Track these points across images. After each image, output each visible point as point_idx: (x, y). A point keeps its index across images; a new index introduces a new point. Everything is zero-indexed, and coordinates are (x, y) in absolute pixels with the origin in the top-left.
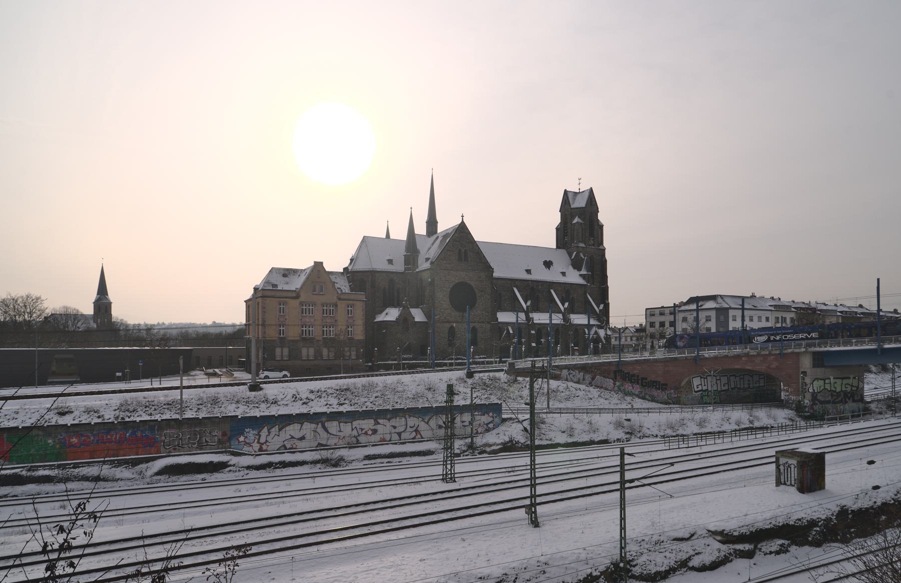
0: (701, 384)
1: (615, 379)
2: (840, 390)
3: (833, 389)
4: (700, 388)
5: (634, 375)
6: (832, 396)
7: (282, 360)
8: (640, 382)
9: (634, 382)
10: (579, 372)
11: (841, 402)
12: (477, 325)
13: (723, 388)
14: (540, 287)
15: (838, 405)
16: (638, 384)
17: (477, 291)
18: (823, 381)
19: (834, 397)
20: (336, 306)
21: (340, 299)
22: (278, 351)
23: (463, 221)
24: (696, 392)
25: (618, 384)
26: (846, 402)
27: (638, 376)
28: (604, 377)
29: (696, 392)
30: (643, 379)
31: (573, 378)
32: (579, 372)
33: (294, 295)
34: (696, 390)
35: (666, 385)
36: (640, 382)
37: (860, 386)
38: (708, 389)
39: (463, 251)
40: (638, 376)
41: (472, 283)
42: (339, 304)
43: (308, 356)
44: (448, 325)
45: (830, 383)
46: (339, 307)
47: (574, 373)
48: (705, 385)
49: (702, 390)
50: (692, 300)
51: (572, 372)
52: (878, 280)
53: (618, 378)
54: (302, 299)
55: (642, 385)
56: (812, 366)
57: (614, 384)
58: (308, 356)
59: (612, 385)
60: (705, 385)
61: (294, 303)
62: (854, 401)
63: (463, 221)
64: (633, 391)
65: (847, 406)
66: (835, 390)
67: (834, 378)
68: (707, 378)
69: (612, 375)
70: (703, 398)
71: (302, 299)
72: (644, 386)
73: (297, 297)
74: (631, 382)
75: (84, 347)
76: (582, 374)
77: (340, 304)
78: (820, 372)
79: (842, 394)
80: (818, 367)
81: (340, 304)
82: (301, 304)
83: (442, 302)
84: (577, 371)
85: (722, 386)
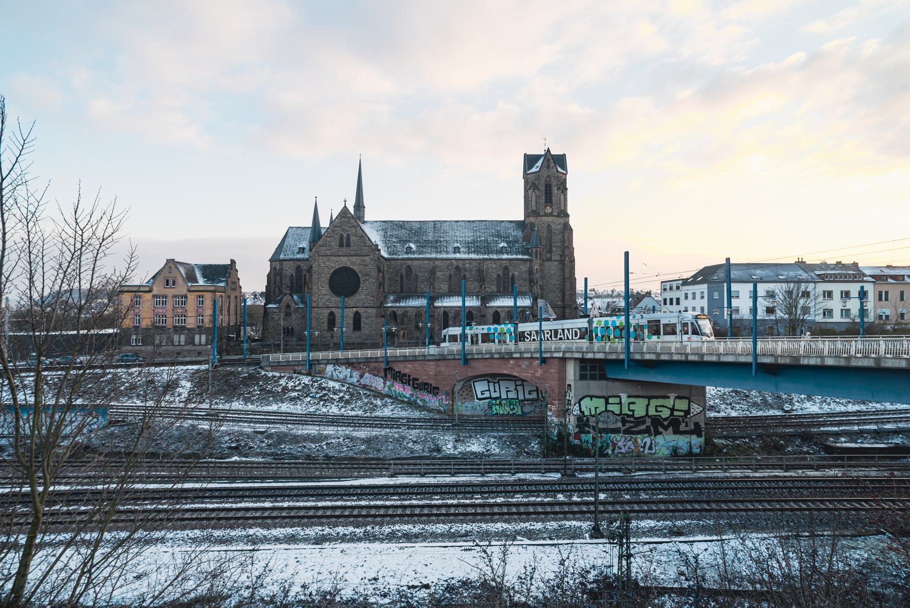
0: (489, 390)
1: (385, 378)
2: (644, 413)
3: (625, 411)
4: (487, 395)
5: (405, 375)
6: (624, 422)
7: (179, 345)
8: (411, 382)
9: (405, 383)
10: (346, 368)
11: (647, 431)
12: (361, 310)
13: (528, 396)
14: (467, 265)
15: (639, 436)
16: (409, 385)
17: (360, 275)
18: (603, 401)
19: (628, 425)
20: (186, 297)
21: (190, 291)
22: (197, 338)
23: (345, 207)
24: (480, 399)
25: (388, 383)
26: (657, 433)
27: (409, 376)
28: (373, 375)
29: (480, 399)
30: (415, 379)
31: (339, 374)
32: (346, 368)
33: (147, 289)
34: (480, 396)
35: (437, 388)
36: (411, 382)
37: (692, 410)
38: (500, 397)
39: (345, 236)
40: (409, 376)
41: (355, 268)
42: (188, 296)
43: (179, 342)
44: (327, 312)
45: (620, 403)
46: (189, 298)
47: (340, 369)
48: (495, 391)
49: (490, 398)
50: (706, 275)
51: (338, 368)
52: (627, 254)
53: (389, 376)
54: (155, 292)
55: (413, 386)
56: (578, 377)
57: (385, 384)
58: (179, 342)
59: (382, 384)
60: (495, 391)
61: (148, 296)
62: (677, 432)
63: (345, 207)
64: (404, 393)
65: (659, 439)
66: (631, 413)
67: (629, 397)
68: (498, 382)
69: (382, 374)
70: (492, 408)
71: (155, 292)
72: (415, 388)
73: (150, 291)
74: (403, 383)
75: (101, 328)
76: (349, 370)
77: (189, 295)
78: (595, 386)
79: (649, 422)
80: (593, 378)
81: (189, 295)
82: (154, 296)
83: (320, 288)
84: (344, 367)
85: (527, 393)
